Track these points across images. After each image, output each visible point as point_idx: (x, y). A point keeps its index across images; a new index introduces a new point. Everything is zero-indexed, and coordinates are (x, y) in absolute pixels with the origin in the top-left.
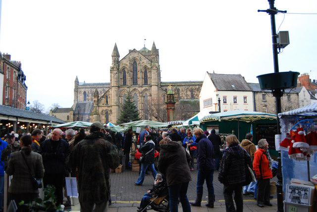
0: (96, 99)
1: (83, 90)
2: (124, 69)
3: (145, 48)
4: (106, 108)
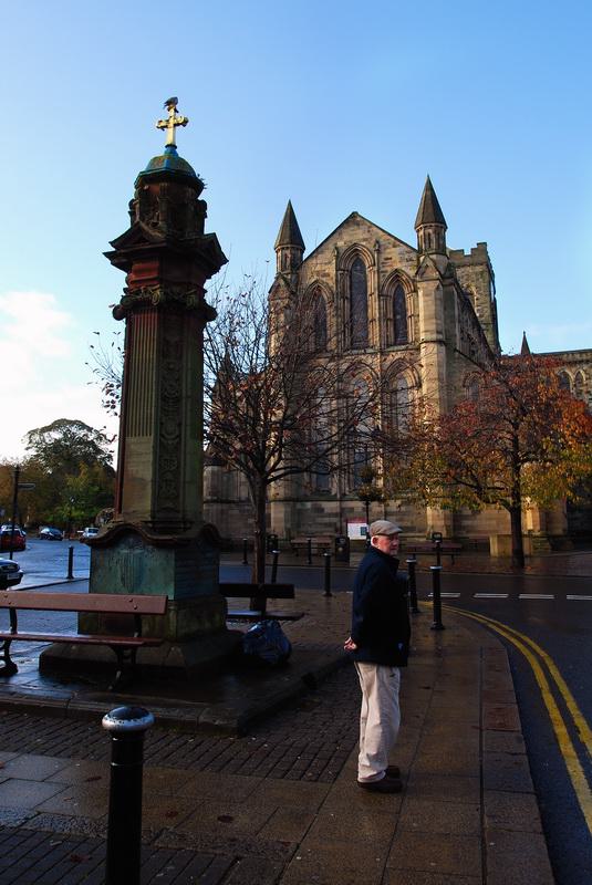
2: (316, 289)
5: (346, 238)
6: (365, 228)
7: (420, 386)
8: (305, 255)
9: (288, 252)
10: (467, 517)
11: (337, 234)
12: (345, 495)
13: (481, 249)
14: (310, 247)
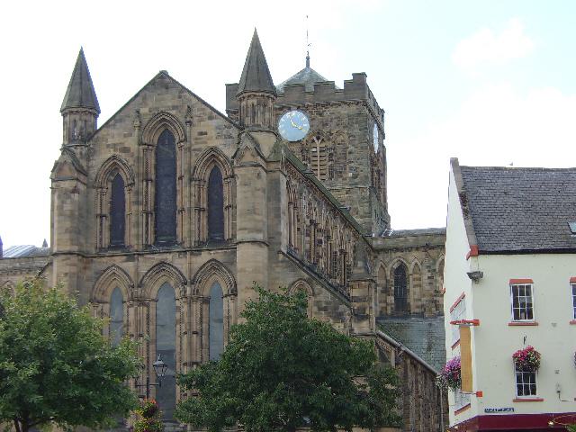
2: (114, 166)
3: (307, 71)
5: (151, 104)
6: (175, 92)
7: (236, 295)
8: (101, 121)
9: (77, 117)
11: (140, 99)
13: (359, 82)
14: (109, 105)
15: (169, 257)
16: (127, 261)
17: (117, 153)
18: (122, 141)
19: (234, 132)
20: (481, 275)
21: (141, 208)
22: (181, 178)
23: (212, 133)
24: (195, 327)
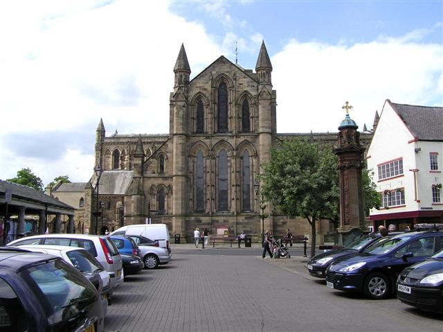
0: (138, 161)
1: (112, 148)
2: (199, 97)
4: (160, 181)
9: (183, 74)
10: (280, 226)
11: (212, 67)
12: (213, 213)
15: (226, 138)
16: (206, 138)
17: (201, 91)
18: (204, 85)
19: (256, 84)
20: (420, 149)
21: (212, 116)
22: (231, 103)
23: (245, 84)
24: (238, 170)
